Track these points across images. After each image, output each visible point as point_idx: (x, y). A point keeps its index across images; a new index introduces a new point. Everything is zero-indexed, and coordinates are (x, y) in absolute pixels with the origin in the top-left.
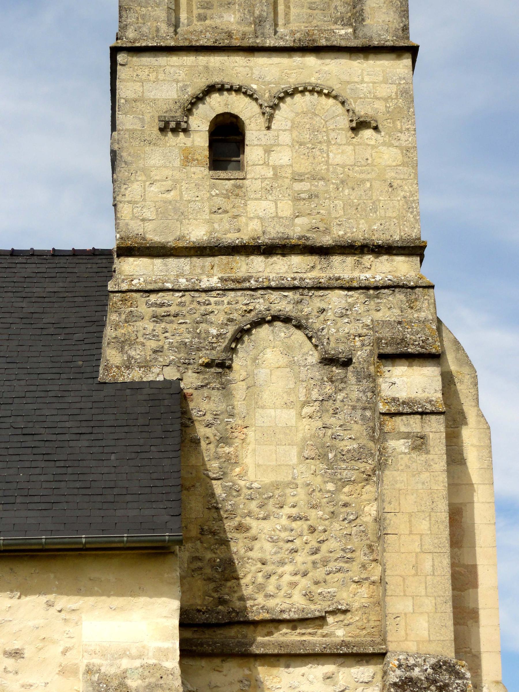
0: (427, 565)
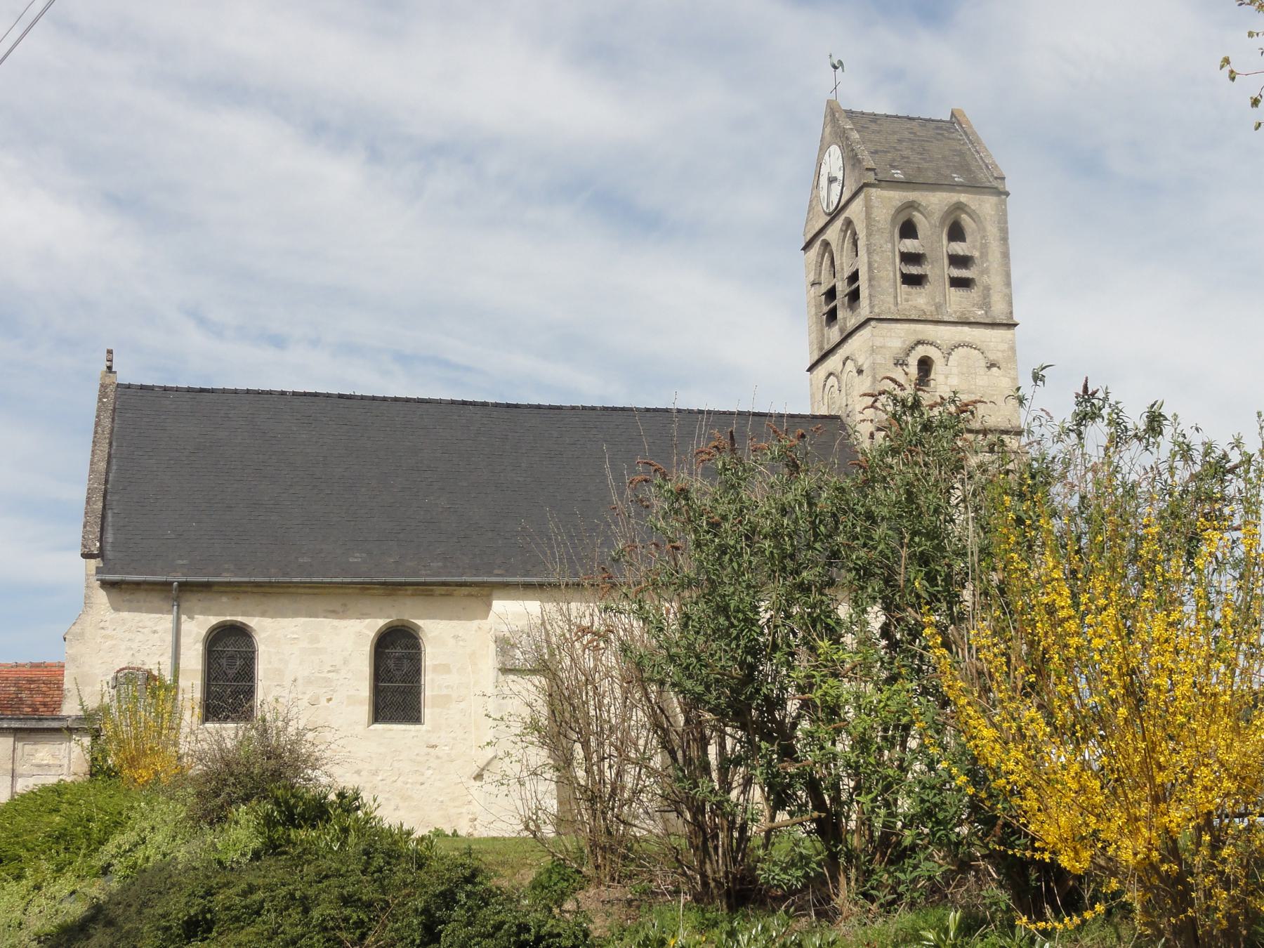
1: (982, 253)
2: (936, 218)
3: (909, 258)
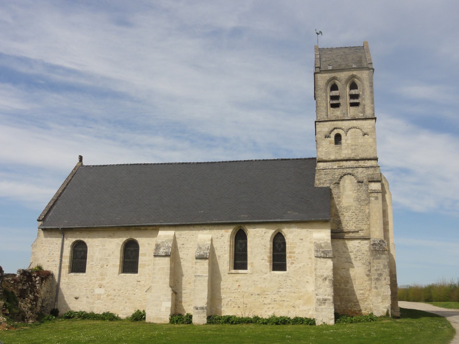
0: (378, 222)
2: (343, 82)
3: (333, 98)
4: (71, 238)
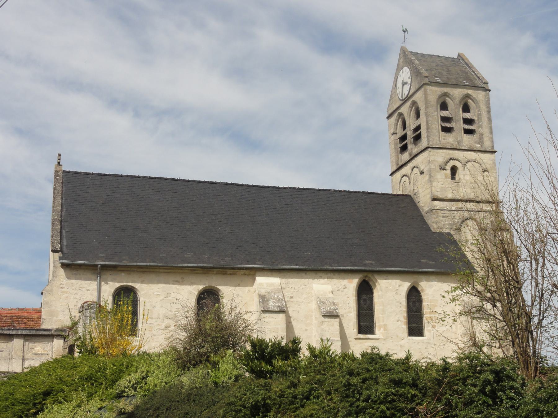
1: (478, 118)
2: (457, 101)
3: (445, 119)
4: (112, 281)
